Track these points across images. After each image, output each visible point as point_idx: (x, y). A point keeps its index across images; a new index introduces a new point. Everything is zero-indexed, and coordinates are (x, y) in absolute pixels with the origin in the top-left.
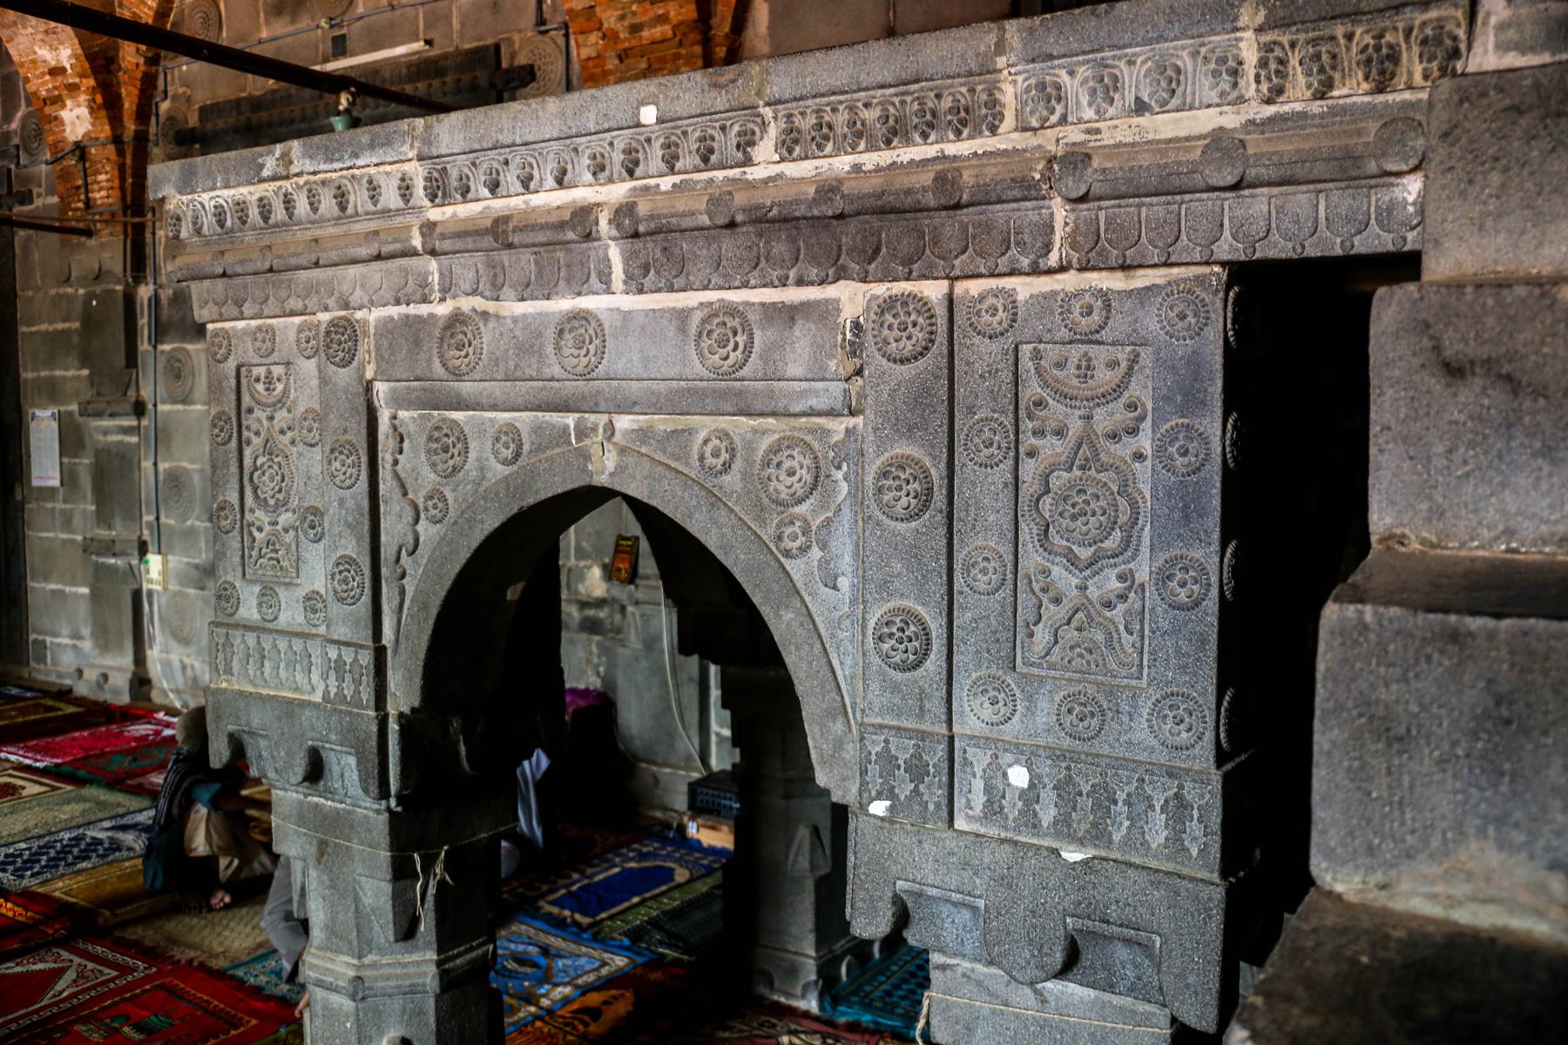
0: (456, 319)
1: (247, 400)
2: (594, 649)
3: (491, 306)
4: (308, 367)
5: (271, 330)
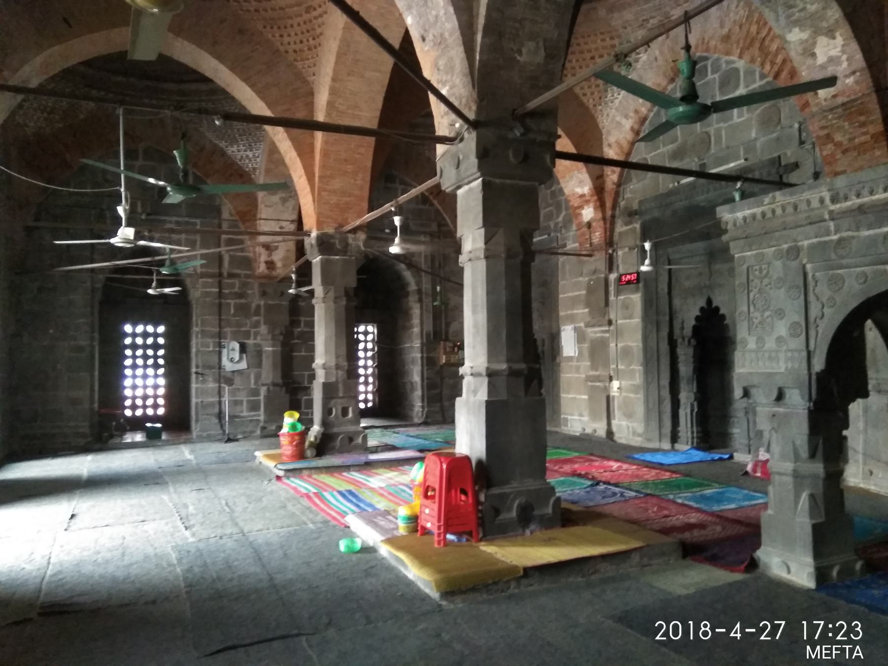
0: (840, 241)
1: (751, 277)
3: (855, 234)
4: (778, 264)
5: (763, 254)
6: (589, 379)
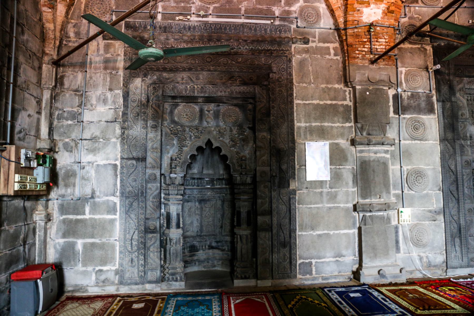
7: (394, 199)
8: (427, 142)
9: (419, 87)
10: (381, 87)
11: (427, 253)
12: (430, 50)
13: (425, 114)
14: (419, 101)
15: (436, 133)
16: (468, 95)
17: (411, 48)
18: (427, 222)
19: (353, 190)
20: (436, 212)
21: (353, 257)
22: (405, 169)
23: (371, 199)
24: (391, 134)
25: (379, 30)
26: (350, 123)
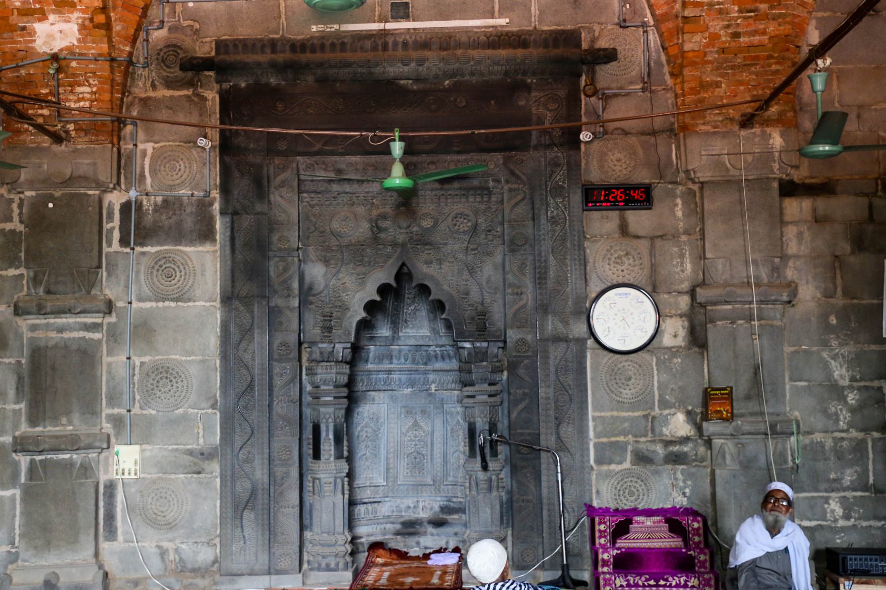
2: (679, 476)
6: (21, 445)
7: (109, 425)
8: (189, 304)
9: (181, 185)
10: (82, 191)
11: (177, 542)
12: (213, 99)
13: (191, 243)
14: (180, 215)
15: (215, 285)
16: (313, 195)
17: (172, 97)
18: (182, 476)
19: (17, 407)
20: (202, 454)
21: (8, 548)
22: (138, 363)
23: (45, 427)
24: (110, 289)
25: (75, 68)
26: (18, 268)
